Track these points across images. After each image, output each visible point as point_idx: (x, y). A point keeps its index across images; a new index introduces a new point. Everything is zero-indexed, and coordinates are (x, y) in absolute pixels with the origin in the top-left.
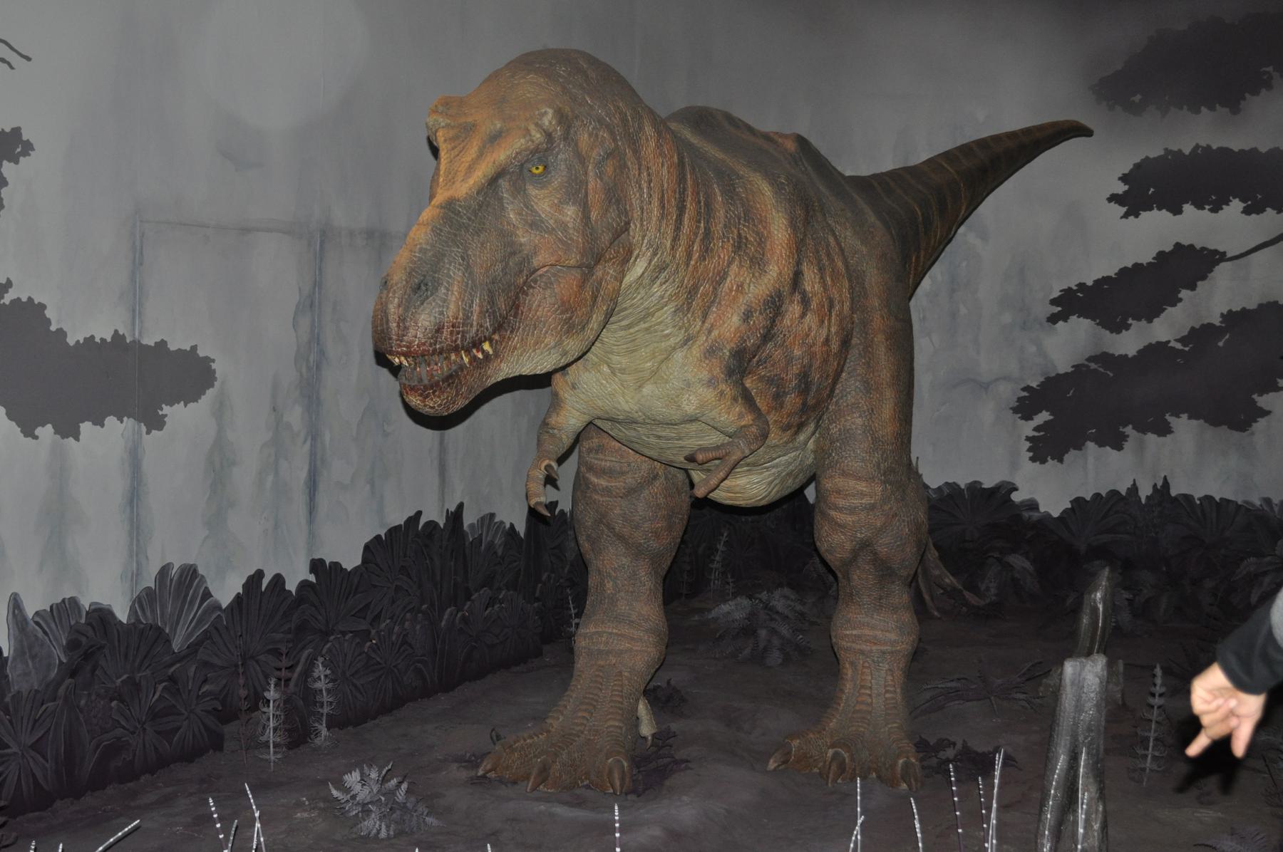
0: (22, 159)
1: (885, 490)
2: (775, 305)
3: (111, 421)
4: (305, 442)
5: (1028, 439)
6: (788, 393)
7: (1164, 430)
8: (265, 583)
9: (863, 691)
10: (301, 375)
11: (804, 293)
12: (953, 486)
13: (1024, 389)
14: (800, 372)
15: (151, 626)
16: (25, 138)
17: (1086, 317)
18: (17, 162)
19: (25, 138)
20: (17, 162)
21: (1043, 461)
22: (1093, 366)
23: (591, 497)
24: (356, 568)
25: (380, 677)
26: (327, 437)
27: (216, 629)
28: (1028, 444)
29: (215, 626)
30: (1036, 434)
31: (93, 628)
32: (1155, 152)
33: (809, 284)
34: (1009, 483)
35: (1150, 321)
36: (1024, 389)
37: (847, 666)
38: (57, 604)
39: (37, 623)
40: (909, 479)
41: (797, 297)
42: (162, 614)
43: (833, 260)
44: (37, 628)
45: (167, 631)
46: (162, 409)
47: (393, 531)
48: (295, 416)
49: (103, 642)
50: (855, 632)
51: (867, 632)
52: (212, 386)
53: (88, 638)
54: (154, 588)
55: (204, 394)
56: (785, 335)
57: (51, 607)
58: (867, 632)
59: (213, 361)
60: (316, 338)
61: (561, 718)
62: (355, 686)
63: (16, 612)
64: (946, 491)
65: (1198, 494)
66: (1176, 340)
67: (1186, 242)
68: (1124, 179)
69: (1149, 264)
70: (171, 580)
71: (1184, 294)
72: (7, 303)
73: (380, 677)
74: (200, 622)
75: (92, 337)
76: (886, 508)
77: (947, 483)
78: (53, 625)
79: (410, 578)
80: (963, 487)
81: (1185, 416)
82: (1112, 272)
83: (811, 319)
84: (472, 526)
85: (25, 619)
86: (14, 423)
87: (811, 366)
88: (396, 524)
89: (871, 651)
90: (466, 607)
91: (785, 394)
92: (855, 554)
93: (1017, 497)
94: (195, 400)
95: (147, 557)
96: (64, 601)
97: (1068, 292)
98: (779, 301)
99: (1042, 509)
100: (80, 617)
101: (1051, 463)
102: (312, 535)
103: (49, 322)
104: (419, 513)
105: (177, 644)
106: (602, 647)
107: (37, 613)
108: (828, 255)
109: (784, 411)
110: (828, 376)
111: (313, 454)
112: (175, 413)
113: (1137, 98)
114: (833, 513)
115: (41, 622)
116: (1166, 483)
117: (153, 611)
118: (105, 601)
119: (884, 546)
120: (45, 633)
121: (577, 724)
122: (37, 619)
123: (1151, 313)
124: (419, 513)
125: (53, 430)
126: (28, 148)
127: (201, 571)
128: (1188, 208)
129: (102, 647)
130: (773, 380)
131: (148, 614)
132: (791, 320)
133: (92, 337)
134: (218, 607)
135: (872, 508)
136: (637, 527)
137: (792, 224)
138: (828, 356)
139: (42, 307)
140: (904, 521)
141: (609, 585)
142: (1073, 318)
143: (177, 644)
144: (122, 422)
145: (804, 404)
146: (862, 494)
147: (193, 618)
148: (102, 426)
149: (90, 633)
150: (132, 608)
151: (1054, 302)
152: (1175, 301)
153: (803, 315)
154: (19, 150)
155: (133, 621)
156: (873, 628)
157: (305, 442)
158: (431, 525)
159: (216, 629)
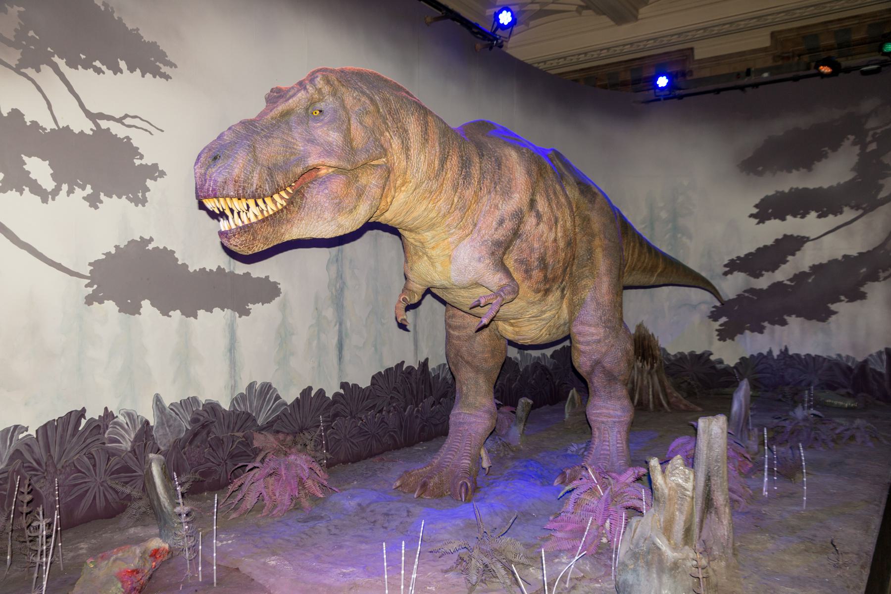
0: (158, 179)
1: (605, 331)
2: (519, 217)
3: (217, 310)
4: (335, 325)
5: (717, 330)
6: (533, 270)
7: (784, 323)
8: (313, 393)
9: (604, 443)
10: (332, 293)
11: (538, 212)
12: (681, 353)
13: (713, 307)
14: (539, 257)
15: (244, 412)
16: (160, 169)
17: (742, 272)
18: (156, 180)
19: (160, 169)
20: (156, 180)
21: (725, 340)
22: (746, 295)
23: (452, 342)
24: (367, 388)
25: (368, 438)
26: (348, 324)
27: (284, 414)
28: (717, 333)
29: (283, 413)
30: (721, 328)
31: (207, 412)
32: (771, 192)
33: (541, 208)
34: (709, 351)
35: (773, 271)
36: (713, 307)
37: (596, 430)
38: (184, 400)
39: (171, 409)
40: (621, 326)
41: (534, 214)
42: (251, 406)
43: (559, 197)
44: (172, 411)
45: (254, 415)
46: (248, 306)
47: (388, 370)
48: (329, 313)
49: (214, 420)
50: (598, 411)
51: (605, 411)
52: (279, 296)
53: (204, 417)
55: (274, 299)
56: (527, 235)
57: (181, 401)
58: (605, 411)
59: (279, 284)
60: (340, 276)
61: (439, 458)
62: (353, 443)
63: (158, 403)
64: (679, 356)
65: (803, 353)
66: (788, 280)
67: (789, 233)
68: (756, 206)
69: (772, 245)
70: (256, 390)
71: (790, 258)
72: (151, 249)
73: (368, 438)
74: (274, 411)
75: (204, 269)
76: (607, 341)
77: (679, 353)
78: (182, 411)
79: (399, 392)
80: (686, 354)
81: (794, 316)
82: (753, 250)
83: (543, 227)
84: (433, 369)
85: (164, 407)
86: (155, 309)
87: (546, 254)
88: (390, 367)
89: (607, 422)
90: (420, 405)
91: (532, 270)
92: (593, 368)
93: (712, 358)
94: (269, 302)
95: (241, 378)
96: (188, 398)
97: (732, 261)
98: (521, 214)
99: (726, 363)
100: (199, 406)
101: (728, 341)
102: (341, 370)
103: (177, 260)
104: (403, 362)
105: (260, 422)
106: (461, 420)
107: (172, 404)
108: (555, 193)
109: (533, 280)
110: (559, 261)
111: (340, 332)
112: (256, 309)
113: (760, 168)
114: (578, 345)
116: (786, 349)
117: (245, 405)
118: (214, 398)
119: (608, 363)
120: (177, 414)
121: (445, 462)
122: (172, 407)
123: (774, 268)
124: (403, 362)
125: (180, 313)
126: (162, 174)
127: (274, 386)
128: (789, 218)
129: (213, 422)
130: (523, 261)
131: (242, 406)
132: (530, 226)
133: (204, 269)
134: (286, 404)
135: (599, 341)
136: (475, 357)
137: (529, 173)
138: (557, 249)
139: (173, 252)
140: (618, 349)
141: (464, 388)
142: (735, 273)
143: (260, 422)
144: (224, 311)
145: (545, 276)
146: (593, 334)
148: (212, 312)
149: (206, 415)
150: (232, 404)
151: (726, 266)
152: (785, 262)
153: (538, 224)
154: (157, 174)
155: (232, 409)
156: (608, 409)
157: (335, 325)
158: (410, 369)
159: (284, 414)
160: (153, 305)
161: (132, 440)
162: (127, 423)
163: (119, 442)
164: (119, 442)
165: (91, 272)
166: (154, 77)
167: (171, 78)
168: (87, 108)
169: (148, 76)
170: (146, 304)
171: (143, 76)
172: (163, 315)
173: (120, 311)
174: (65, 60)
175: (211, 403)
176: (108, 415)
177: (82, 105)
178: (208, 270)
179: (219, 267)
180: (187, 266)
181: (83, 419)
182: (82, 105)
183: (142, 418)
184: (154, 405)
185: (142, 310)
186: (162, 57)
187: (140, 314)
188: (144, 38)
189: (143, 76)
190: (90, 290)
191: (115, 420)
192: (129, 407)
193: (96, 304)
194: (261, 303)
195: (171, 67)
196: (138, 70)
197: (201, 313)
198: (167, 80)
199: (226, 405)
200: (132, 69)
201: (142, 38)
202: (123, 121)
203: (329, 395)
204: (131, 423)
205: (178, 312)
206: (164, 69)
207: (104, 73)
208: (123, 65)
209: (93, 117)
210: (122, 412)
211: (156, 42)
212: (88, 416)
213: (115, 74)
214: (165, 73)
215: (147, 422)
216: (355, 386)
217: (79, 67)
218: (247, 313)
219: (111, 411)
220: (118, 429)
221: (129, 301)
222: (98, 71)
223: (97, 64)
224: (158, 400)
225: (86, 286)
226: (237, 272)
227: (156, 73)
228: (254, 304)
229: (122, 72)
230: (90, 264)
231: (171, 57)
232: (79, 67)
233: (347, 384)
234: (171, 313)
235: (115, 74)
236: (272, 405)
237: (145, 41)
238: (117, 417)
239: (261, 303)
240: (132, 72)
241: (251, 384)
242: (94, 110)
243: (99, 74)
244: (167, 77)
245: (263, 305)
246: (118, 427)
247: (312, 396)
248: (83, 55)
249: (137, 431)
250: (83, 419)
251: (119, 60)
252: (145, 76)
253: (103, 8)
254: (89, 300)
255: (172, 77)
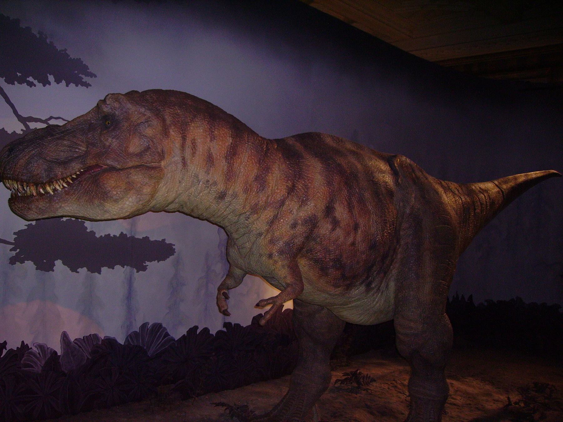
3: (118, 267)
38: (86, 337)
54: (138, 332)
55: (169, 257)
63: (65, 338)
70: (148, 330)
75: (109, 235)
78: (84, 344)
96: (90, 335)
100: (99, 342)
105: (150, 353)
107: (76, 339)
112: (152, 265)
115: (77, 342)
122: (76, 341)
125: (87, 270)
127: (164, 325)
131: (135, 342)
133: (109, 235)
134: (174, 340)
143: (150, 353)
144: (124, 267)
147: (159, 343)
148: (113, 269)
150: (127, 339)
160: (64, 263)
161: (42, 366)
162: (39, 353)
163: (32, 367)
164: (32, 367)
165: (15, 239)
166: (77, 86)
167: (90, 86)
168: (20, 113)
169: (72, 85)
170: (59, 263)
171: (67, 86)
172: (72, 271)
173: (37, 269)
174: (4, 78)
175: (109, 339)
176: (24, 347)
177: (15, 112)
178: (112, 235)
179: (122, 233)
180: (95, 233)
181: (4, 349)
182: (15, 112)
183: (52, 349)
184: (62, 340)
185: (55, 268)
186: (85, 70)
187: (53, 271)
188: (71, 57)
189: (67, 86)
190: (14, 253)
191: (30, 350)
192: (40, 341)
193: (18, 263)
194: (156, 261)
195: (91, 77)
196: (64, 82)
197: (104, 269)
198: (87, 88)
199: (121, 340)
200: (58, 81)
201: (69, 56)
202: (48, 122)
203: (213, 332)
204: (42, 353)
205: (85, 269)
206: (86, 79)
207: (35, 86)
208: (51, 78)
209: (23, 120)
210: (35, 345)
211: (80, 59)
212: (9, 347)
213: (44, 86)
214: (86, 82)
215: (55, 353)
216: (238, 325)
217: (16, 83)
218: (144, 269)
219: (27, 344)
220: (32, 357)
221: (45, 261)
222: (31, 84)
223: (31, 79)
224: (65, 336)
225: (11, 250)
226: (137, 237)
227: (79, 82)
228: (151, 261)
229: (50, 84)
230: (15, 233)
231: (91, 69)
232: (16, 83)
233: (230, 323)
234: (79, 270)
235: (44, 86)
236: (161, 341)
237: (71, 58)
238: (31, 348)
239: (156, 261)
240: (58, 83)
241: (144, 324)
242: (25, 115)
243: (31, 87)
244: (87, 85)
245: (158, 262)
246: (32, 356)
247: (198, 333)
248: (20, 73)
249: (47, 359)
250: (4, 349)
251: (48, 75)
252: (69, 85)
253: (38, 36)
254: (13, 261)
255: (92, 85)
